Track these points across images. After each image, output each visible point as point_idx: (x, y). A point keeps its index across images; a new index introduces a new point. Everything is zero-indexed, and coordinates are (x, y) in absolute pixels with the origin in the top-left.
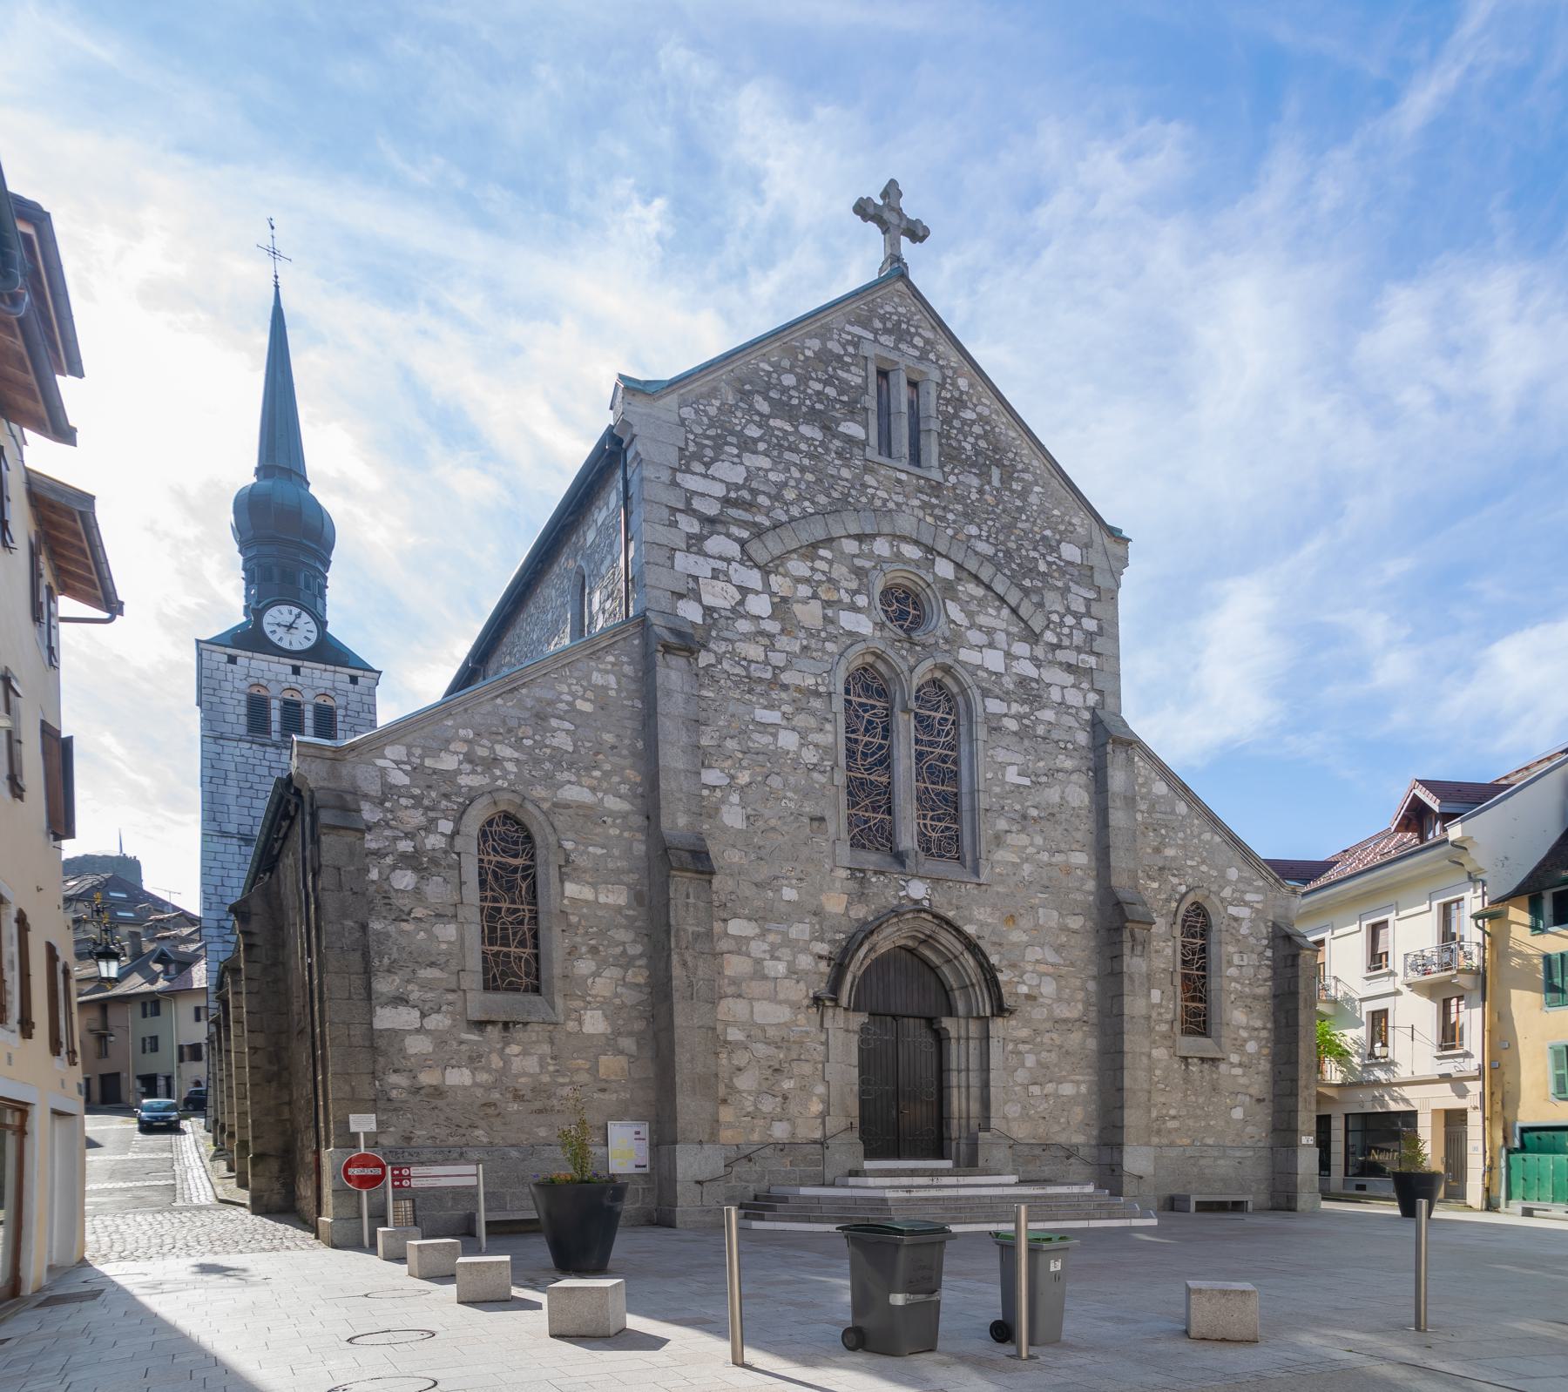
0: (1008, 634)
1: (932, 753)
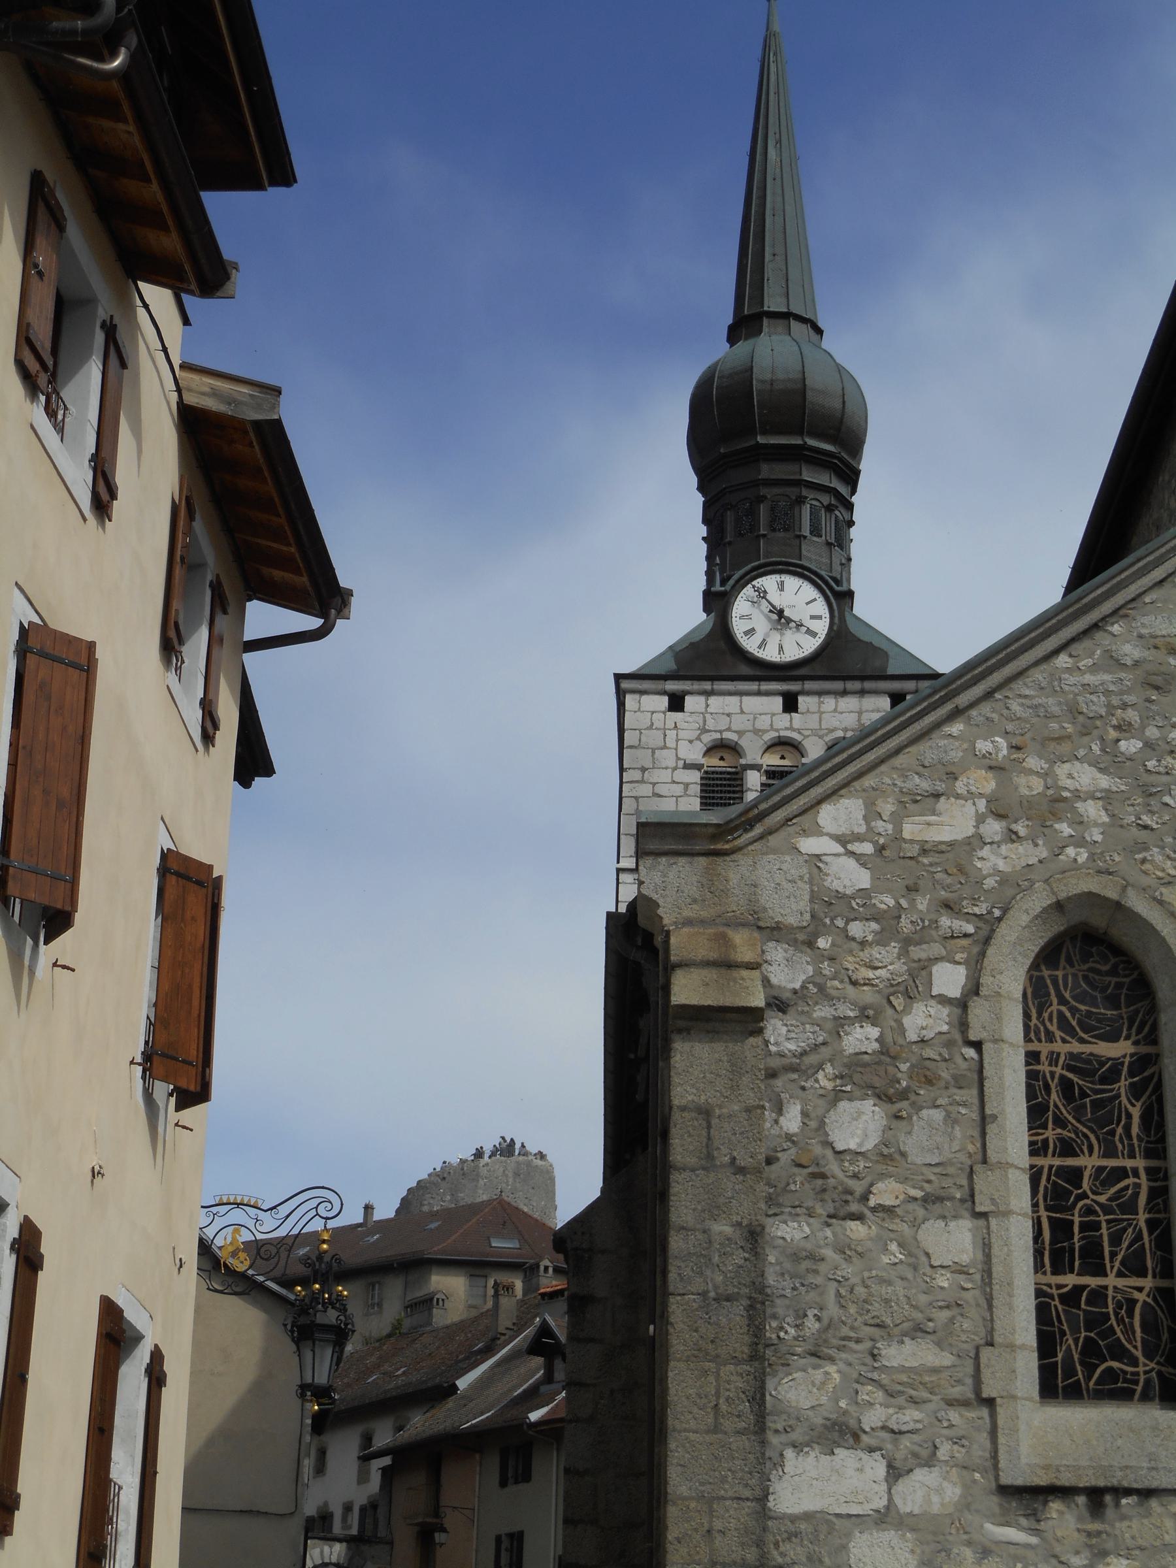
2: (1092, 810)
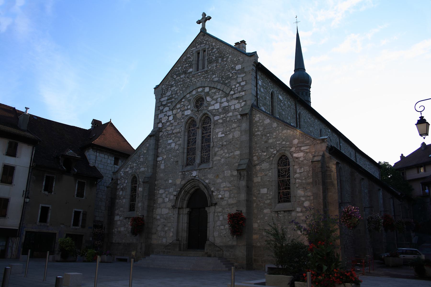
0: (221, 97)
2: (135, 167)
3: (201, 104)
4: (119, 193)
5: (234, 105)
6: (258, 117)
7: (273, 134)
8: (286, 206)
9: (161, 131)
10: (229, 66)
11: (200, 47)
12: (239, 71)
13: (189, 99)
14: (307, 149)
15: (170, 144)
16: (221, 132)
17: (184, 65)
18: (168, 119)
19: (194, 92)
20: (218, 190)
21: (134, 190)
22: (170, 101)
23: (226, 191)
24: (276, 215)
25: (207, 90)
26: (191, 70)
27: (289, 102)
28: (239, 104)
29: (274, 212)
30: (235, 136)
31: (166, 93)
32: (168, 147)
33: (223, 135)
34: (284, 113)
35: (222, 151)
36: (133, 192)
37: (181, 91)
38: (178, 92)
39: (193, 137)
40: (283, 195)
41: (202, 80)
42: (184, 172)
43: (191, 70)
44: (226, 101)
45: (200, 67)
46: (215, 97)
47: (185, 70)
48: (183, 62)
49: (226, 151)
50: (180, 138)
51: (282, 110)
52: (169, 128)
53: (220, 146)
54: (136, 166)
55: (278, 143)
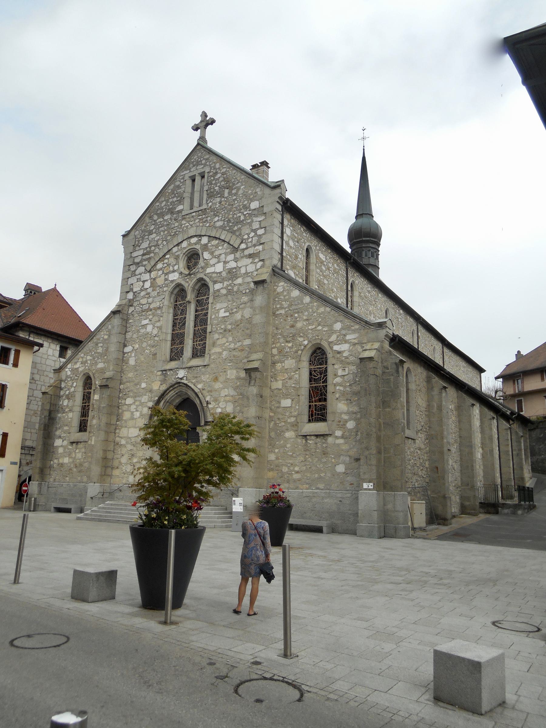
1: (202, 313)
2: (89, 362)
3: (196, 264)
4: (63, 403)
5: (246, 266)
6: (282, 287)
7: (303, 315)
8: (319, 427)
9: (131, 306)
10: (240, 202)
11: (195, 171)
12: (256, 212)
13: (177, 254)
14: (355, 339)
15: (144, 326)
16: (224, 309)
17: (170, 199)
18: (143, 286)
19: (184, 244)
20: (216, 400)
21: (87, 397)
22: (147, 256)
23: (229, 401)
24: (304, 441)
25: (205, 240)
26: (180, 207)
27: (335, 265)
28: (254, 265)
29: (301, 437)
30: (245, 315)
31: (141, 244)
32: (142, 331)
33: (227, 314)
34: (326, 282)
35: (224, 339)
36: (84, 401)
37: (164, 242)
38: (160, 242)
39: (181, 317)
40: (316, 410)
41: (198, 224)
42: (165, 370)
43: (180, 207)
44: (233, 260)
45: (196, 204)
46: (217, 253)
47: (172, 208)
48: (169, 193)
49: (231, 339)
50: (161, 316)
51: (324, 276)
52: (144, 301)
53: (221, 331)
54: (90, 360)
55: (310, 327)
